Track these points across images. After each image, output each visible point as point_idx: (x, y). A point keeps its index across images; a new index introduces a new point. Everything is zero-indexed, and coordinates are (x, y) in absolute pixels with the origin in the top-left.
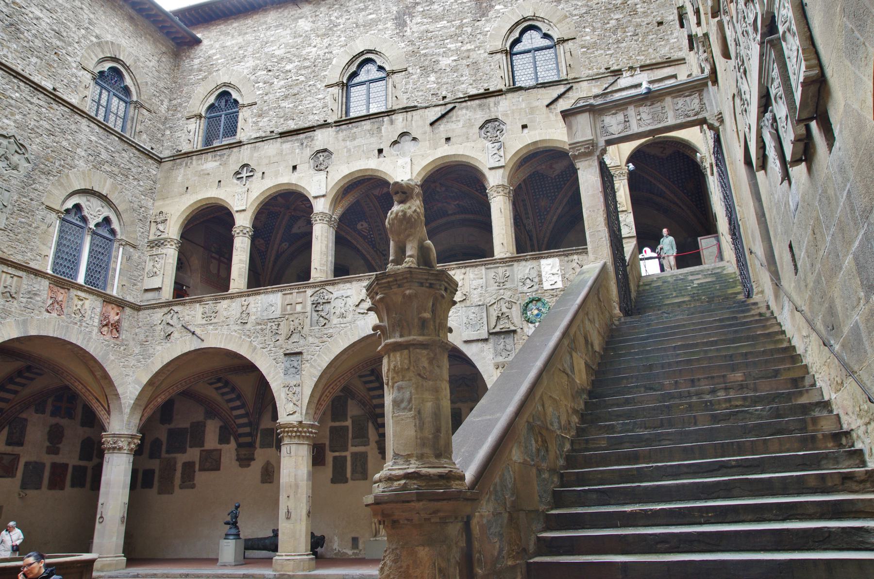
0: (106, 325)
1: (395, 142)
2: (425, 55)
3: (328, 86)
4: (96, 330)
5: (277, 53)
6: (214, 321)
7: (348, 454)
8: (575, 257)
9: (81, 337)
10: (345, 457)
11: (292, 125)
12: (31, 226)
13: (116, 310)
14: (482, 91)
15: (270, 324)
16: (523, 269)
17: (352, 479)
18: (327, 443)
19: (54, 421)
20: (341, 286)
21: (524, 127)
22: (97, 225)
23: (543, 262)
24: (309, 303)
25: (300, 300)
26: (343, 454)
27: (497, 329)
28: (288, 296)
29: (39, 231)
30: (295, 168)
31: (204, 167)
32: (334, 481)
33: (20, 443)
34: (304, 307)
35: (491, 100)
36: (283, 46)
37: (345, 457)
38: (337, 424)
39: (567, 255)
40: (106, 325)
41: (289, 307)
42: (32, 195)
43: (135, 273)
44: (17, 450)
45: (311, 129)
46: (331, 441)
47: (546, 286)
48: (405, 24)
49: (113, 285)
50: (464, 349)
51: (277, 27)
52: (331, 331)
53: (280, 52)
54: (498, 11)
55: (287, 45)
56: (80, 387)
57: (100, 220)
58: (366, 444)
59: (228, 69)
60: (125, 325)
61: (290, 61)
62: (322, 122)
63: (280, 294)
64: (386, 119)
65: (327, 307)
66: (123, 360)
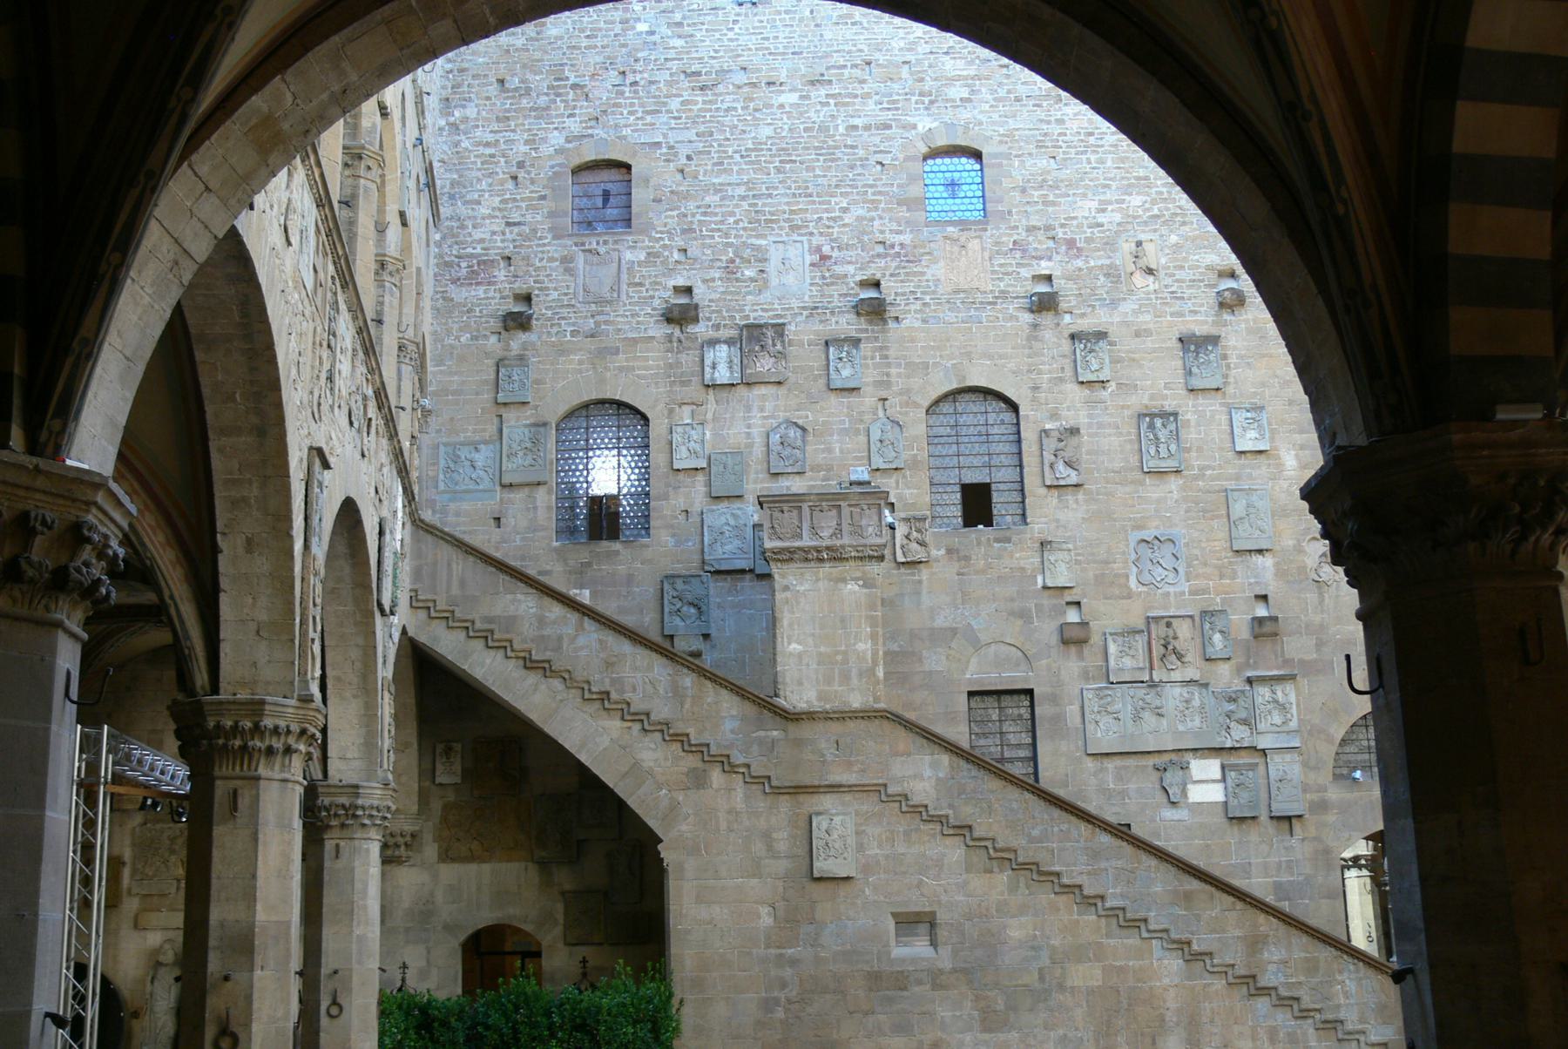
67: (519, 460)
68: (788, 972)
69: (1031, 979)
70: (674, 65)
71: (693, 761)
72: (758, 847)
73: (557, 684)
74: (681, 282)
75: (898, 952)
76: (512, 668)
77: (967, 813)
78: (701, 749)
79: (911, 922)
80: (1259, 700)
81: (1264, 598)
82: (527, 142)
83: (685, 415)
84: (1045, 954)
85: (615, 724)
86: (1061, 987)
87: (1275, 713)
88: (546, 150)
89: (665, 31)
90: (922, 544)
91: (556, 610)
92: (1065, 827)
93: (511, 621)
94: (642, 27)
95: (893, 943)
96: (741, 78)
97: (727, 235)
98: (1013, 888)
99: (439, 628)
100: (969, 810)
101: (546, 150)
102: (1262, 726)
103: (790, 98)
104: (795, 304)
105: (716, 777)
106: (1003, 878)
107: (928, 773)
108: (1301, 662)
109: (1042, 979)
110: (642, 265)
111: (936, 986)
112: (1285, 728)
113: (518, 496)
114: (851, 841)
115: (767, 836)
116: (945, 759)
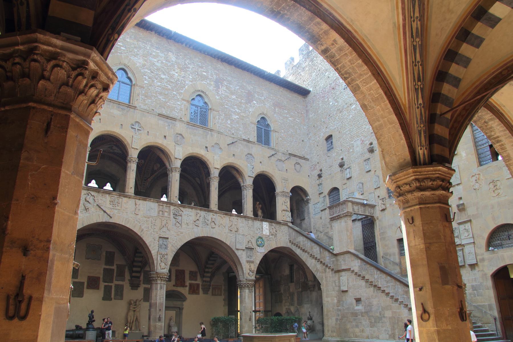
1: (213, 146)
2: (226, 108)
3: (183, 99)
5: (156, 64)
6: (117, 208)
7: (113, 285)
8: (274, 224)
10: (111, 286)
11: (164, 112)
14: (247, 139)
15: (151, 219)
16: (257, 223)
17: (115, 299)
18: (101, 277)
20: (187, 209)
21: (261, 162)
23: (264, 223)
24: (172, 214)
25: (167, 210)
26: (110, 284)
27: (247, 247)
28: (161, 207)
30: (165, 137)
31: (112, 111)
32: (104, 299)
34: (169, 214)
35: (250, 145)
36: (160, 62)
37: (111, 286)
38: (107, 267)
39: (271, 222)
41: (161, 212)
45: (174, 119)
46: (104, 276)
47: (264, 233)
48: (219, 88)
50: (236, 252)
51: (157, 48)
52: (182, 231)
53: (159, 65)
54: (254, 104)
55: (162, 63)
58: (123, 280)
59: (128, 56)
61: (165, 75)
62: (179, 118)
63: (157, 204)
64: (209, 132)
65: (180, 217)
67: (322, 205)
68: (339, 313)
69: (378, 314)
70: (336, 109)
71: (324, 267)
72: (334, 284)
73: (307, 254)
74: (341, 157)
75: (357, 308)
76: (301, 251)
77: (363, 273)
78: (324, 264)
79: (358, 300)
80: (461, 229)
81: (460, 198)
82: (319, 137)
83: (345, 187)
84: (380, 308)
85: (314, 260)
86: (384, 317)
87: (465, 233)
88: (321, 137)
89: (334, 102)
90: (384, 204)
91: (305, 239)
92: (381, 275)
93: (300, 242)
94: (331, 103)
95: (355, 305)
96: (346, 106)
97: (347, 143)
98: (374, 292)
99: (293, 245)
100: (364, 273)
101: (321, 137)
102: (462, 238)
103: (354, 106)
104: (359, 154)
105: (327, 270)
106: (372, 289)
107: (357, 264)
108: (473, 215)
109: (380, 314)
110: (336, 156)
111: (362, 316)
112: (469, 237)
113: (323, 212)
114: (346, 282)
115: (335, 282)
116: (359, 261)
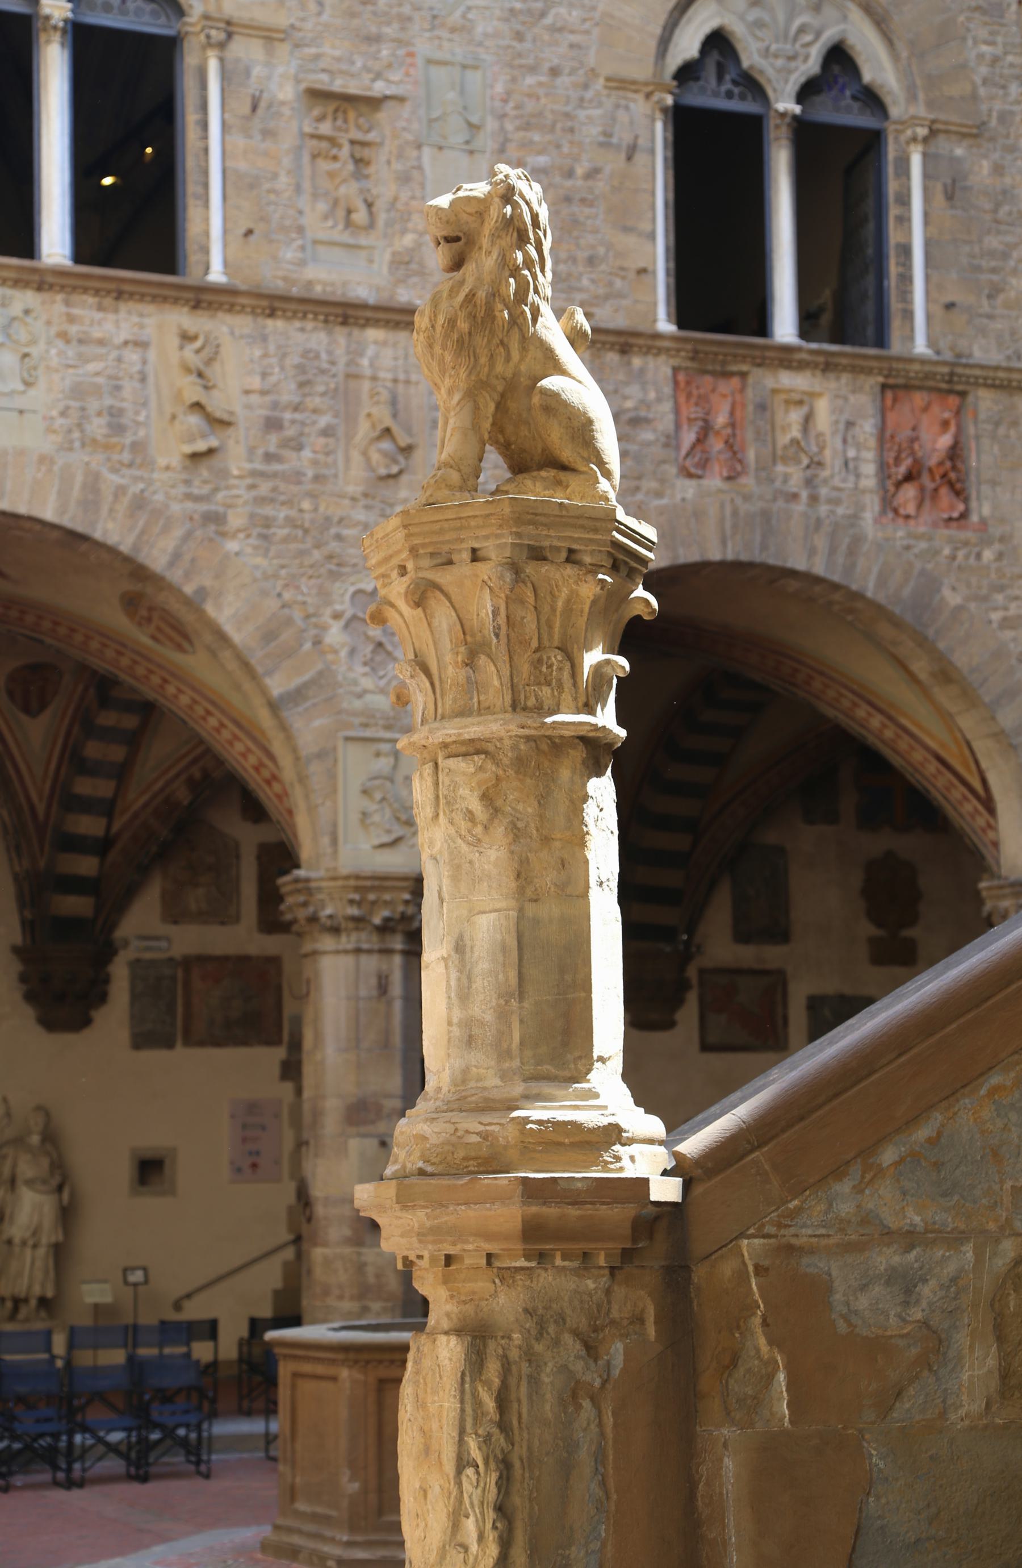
0: (909, 477)
4: (872, 505)
9: (821, 542)
12: (570, 174)
13: (941, 411)
19: (880, 843)
22: (806, 92)
29: (600, 185)
33: (778, 932)
40: (909, 477)
42: (552, 56)
43: (993, 242)
44: (772, 955)
49: (908, 315)
56: (876, 721)
57: (811, 65)
60: (982, 459)
66: (999, 598)
